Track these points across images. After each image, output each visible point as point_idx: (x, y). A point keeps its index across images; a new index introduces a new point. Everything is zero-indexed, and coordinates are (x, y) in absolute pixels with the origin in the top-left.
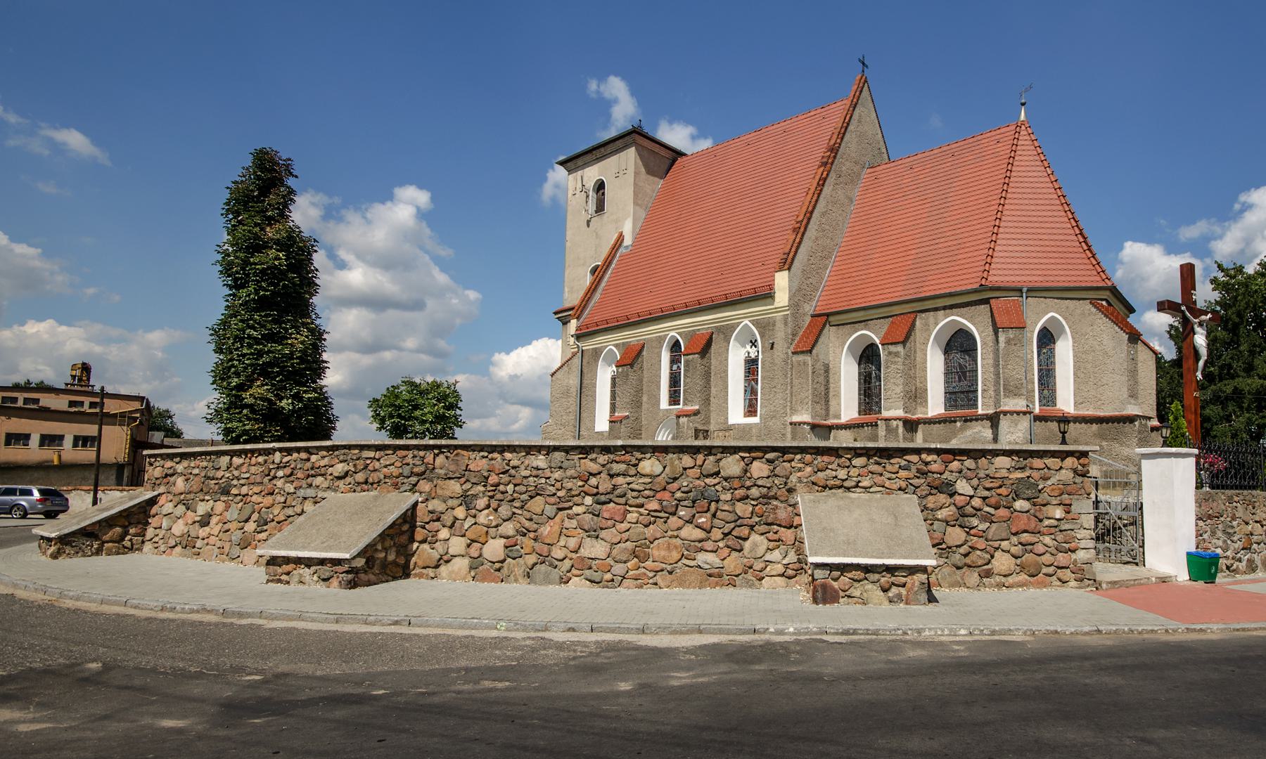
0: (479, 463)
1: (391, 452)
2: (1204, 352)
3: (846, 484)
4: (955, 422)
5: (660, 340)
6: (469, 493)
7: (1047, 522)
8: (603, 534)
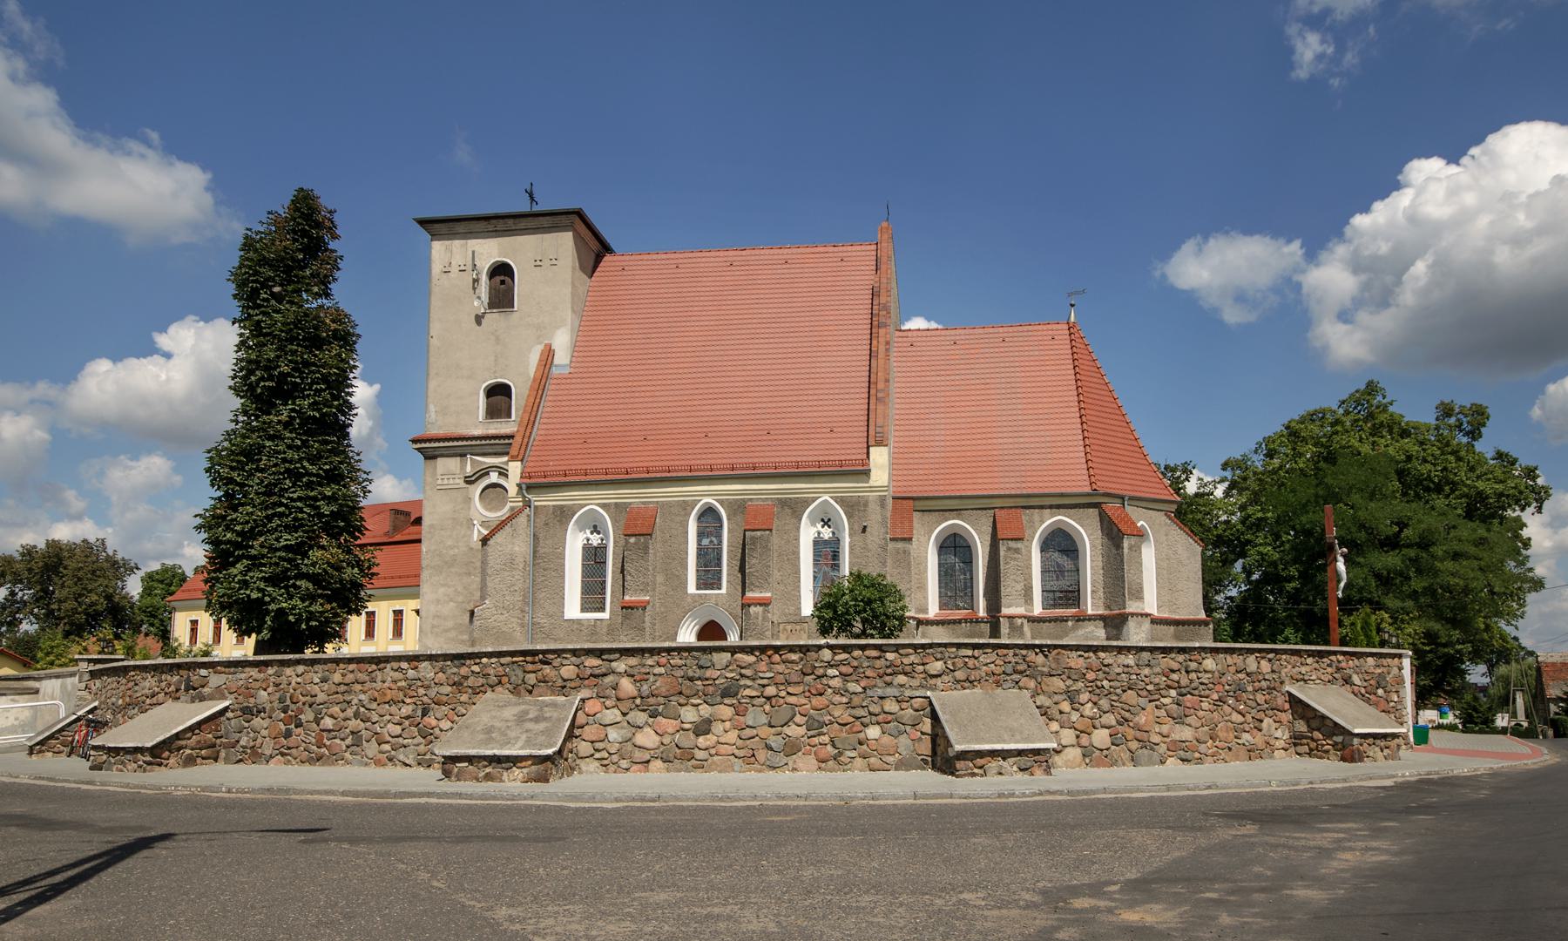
0: (1075, 661)
1: (990, 651)
2: (1344, 576)
3: (1306, 678)
4: (1066, 621)
5: (686, 507)
6: (1072, 689)
7: (1392, 704)
8: (1188, 720)
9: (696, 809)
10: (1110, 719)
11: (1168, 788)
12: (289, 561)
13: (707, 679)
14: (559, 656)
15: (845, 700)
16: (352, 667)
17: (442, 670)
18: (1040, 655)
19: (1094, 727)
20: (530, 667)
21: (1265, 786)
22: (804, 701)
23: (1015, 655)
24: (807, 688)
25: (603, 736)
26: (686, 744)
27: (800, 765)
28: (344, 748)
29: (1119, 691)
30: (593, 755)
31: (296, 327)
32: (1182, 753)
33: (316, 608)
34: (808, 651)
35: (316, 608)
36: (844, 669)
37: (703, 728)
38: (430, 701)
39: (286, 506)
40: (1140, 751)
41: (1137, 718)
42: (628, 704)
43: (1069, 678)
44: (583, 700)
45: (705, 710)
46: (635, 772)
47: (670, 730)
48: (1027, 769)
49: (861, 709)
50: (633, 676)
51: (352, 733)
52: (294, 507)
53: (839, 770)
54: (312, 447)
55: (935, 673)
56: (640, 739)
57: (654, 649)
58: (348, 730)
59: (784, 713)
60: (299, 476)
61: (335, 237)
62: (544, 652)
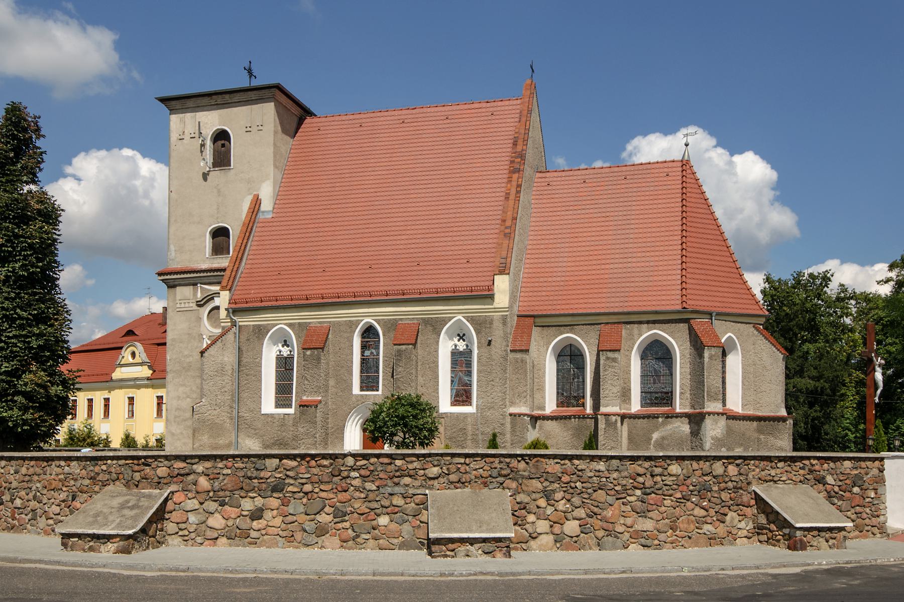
0: (553, 467)
1: (480, 459)
2: (881, 384)
3: (775, 479)
4: (658, 418)
5: (352, 325)
6: (548, 489)
7: (868, 500)
8: (650, 514)
9: (211, 580)
10: (581, 513)
11: (586, 572)
12: (8, 382)
13: (261, 479)
14: (156, 460)
15: (363, 495)
16: (33, 463)
17: (84, 468)
18: (523, 462)
19: (567, 520)
20: (136, 468)
21: (677, 571)
22: (332, 496)
23: (500, 462)
24: (334, 486)
25: (185, 519)
26: (244, 526)
27: (327, 544)
28: (27, 521)
29: (590, 491)
30: (177, 533)
31: (8, 210)
32: (643, 540)
33: (28, 416)
34: (337, 458)
35: (28, 416)
36: (363, 472)
37: (257, 515)
38: (76, 490)
39: (5, 342)
40: (606, 538)
41: (605, 512)
42: (204, 496)
43: (546, 480)
44: (173, 493)
45: (259, 501)
46: (206, 546)
47: (233, 516)
48: (490, 553)
49: (375, 503)
50: (208, 475)
51: (32, 510)
52: (10, 343)
53: (356, 549)
54: (24, 297)
55: (432, 476)
56: (211, 522)
57: (224, 455)
58: (29, 509)
59: (317, 505)
60: (13, 320)
61: (39, 136)
62: (146, 457)
